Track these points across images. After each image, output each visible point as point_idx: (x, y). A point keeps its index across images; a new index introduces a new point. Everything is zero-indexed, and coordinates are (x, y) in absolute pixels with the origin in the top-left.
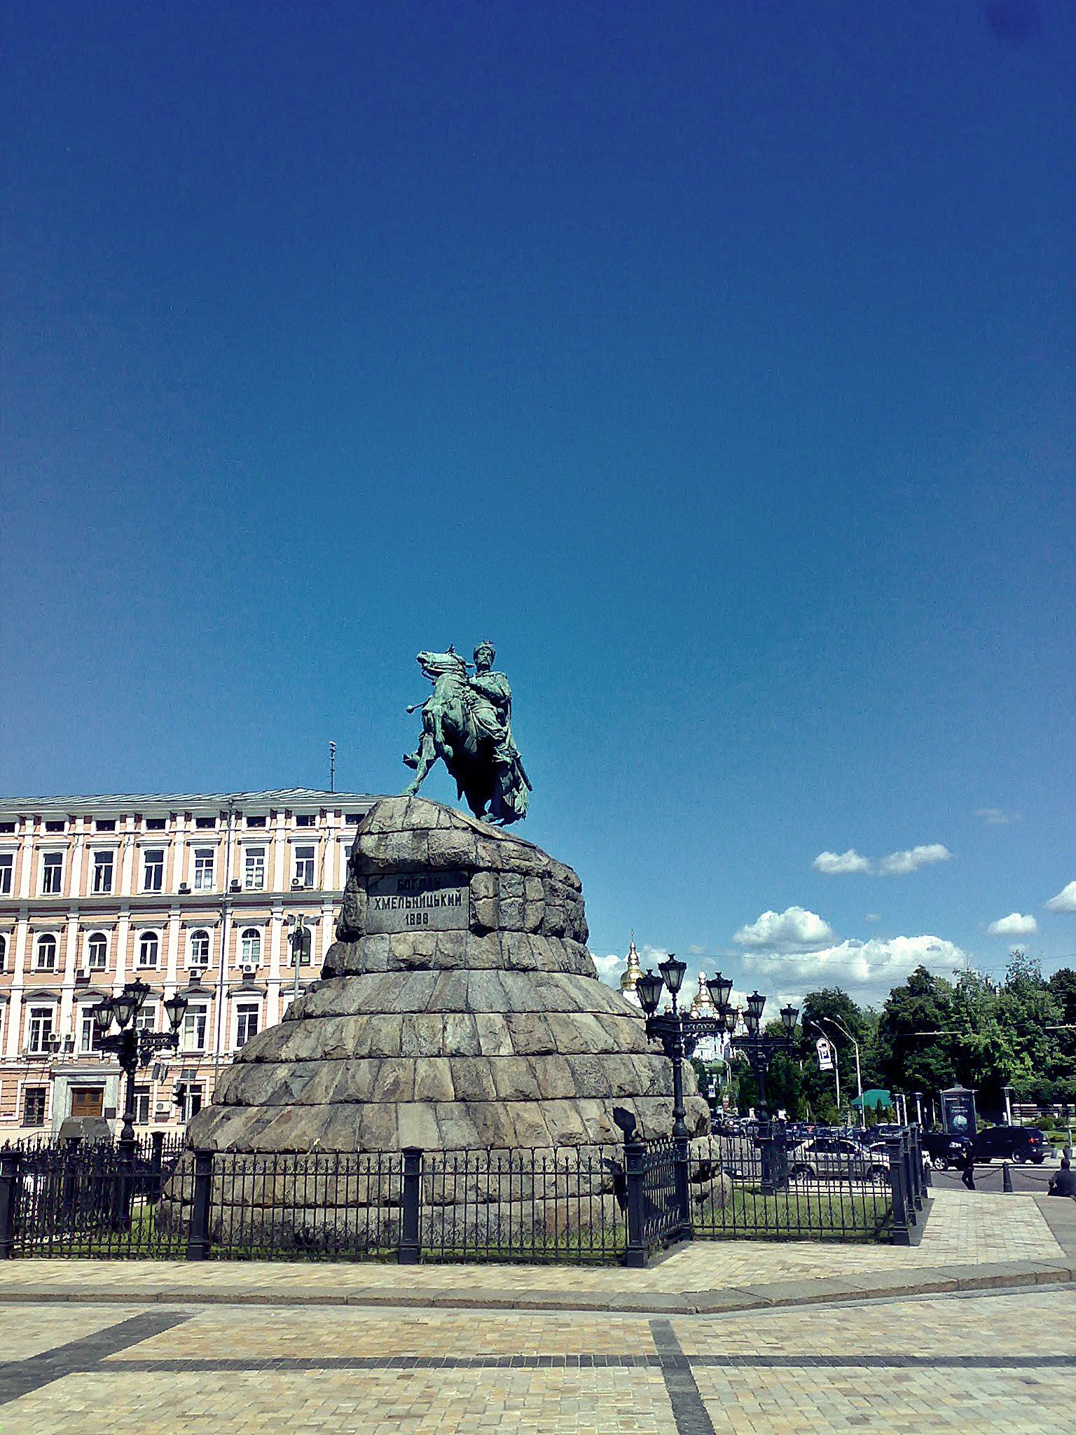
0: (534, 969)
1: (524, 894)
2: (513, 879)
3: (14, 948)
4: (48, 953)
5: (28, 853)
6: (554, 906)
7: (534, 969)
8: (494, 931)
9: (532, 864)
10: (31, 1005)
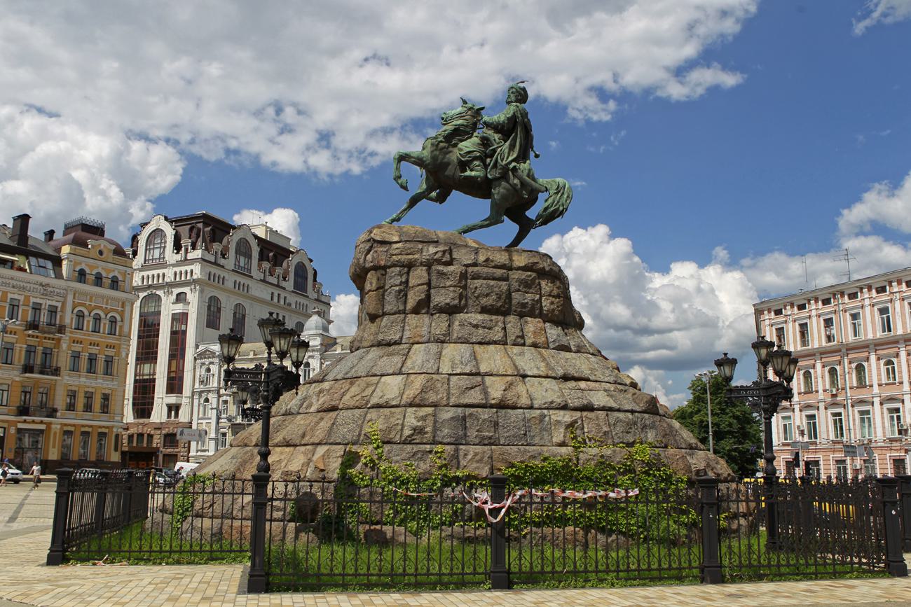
0: (396, 343)
1: (407, 282)
2: (393, 272)
3: (870, 371)
4: (891, 372)
5: (868, 309)
6: (445, 287)
7: (396, 343)
8: (380, 316)
9: (416, 256)
10: (886, 406)
